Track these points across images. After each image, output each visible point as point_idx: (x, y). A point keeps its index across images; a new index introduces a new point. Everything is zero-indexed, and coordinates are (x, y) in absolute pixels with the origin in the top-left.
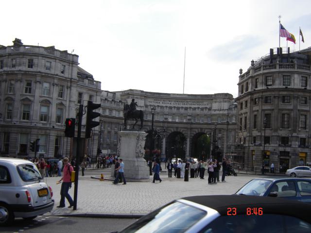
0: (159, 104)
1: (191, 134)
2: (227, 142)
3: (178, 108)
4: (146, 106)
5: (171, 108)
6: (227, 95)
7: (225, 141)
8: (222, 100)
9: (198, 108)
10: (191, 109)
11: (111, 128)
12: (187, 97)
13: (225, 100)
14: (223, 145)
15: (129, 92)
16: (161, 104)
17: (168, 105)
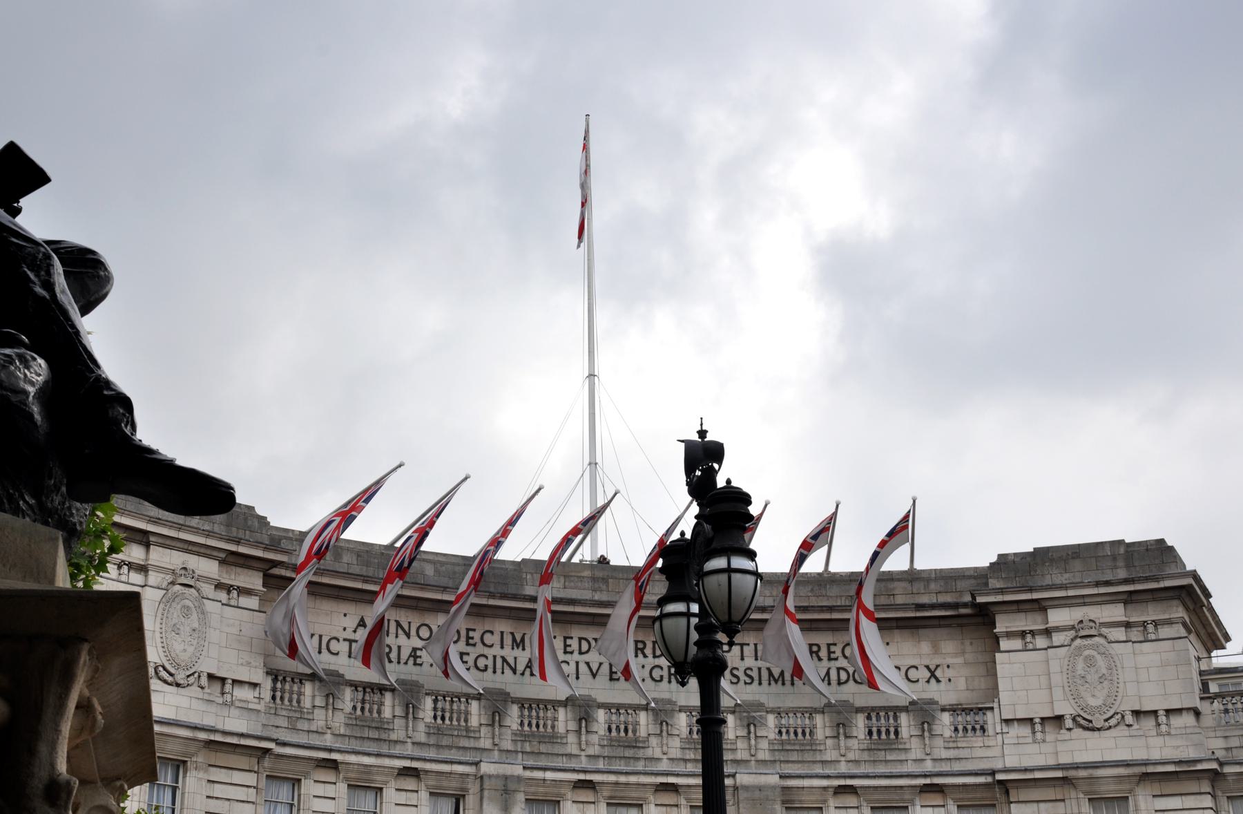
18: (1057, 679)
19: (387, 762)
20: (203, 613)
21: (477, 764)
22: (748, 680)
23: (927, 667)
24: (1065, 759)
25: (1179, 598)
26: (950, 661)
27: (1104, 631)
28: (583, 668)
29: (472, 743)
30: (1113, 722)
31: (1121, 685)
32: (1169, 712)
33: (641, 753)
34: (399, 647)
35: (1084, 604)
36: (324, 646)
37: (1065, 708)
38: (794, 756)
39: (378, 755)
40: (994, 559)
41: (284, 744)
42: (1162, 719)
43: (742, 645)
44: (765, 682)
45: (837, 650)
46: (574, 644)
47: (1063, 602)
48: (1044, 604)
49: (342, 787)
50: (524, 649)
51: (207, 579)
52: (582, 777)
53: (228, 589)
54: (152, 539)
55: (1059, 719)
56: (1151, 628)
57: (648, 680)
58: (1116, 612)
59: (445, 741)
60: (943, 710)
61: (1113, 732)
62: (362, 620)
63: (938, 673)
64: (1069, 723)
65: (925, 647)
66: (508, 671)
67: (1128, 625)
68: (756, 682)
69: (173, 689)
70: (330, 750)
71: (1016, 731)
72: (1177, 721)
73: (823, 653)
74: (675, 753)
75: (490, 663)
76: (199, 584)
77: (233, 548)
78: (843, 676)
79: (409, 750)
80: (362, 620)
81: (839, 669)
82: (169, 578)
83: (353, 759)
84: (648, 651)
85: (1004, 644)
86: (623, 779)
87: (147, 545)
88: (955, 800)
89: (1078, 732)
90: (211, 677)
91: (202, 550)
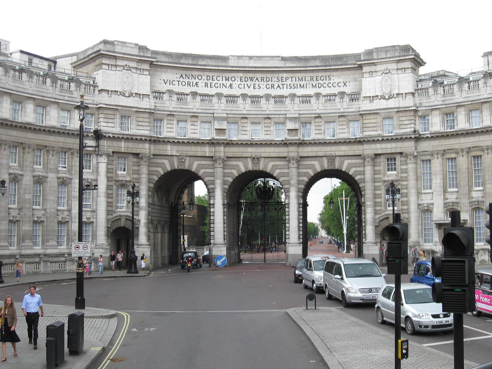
0: (194, 89)
1: (299, 175)
2: (419, 194)
3: (255, 99)
4: (158, 94)
5: (232, 99)
6: (407, 49)
7: (412, 193)
8: (393, 66)
9: (318, 95)
10: (297, 100)
11: (46, 168)
12: (278, 64)
13: (401, 65)
15: (101, 47)
16: (201, 89)
17: (226, 91)
21: (214, 114)
22: (294, 87)
23: (344, 82)
25: (411, 61)
28: (246, 86)
31: (394, 87)
32: (406, 94)
34: (193, 82)
35: (386, 64)
36: (171, 83)
39: (185, 112)
40: (364, 51)
42: (404, 96)
43: (292, 78)
45: (319, 78)
46: (243, 79)
47: (381, 63)
48: (375, 64)
50: (229, 81)
55: (377, 96)
62: (182, 75)
63: (346, 84)
68: (296, 88)
73: (315, 79)
75: (219, 85)
76: (131, 69)
78: (320, 85)
80: (182, 75)
81: (319, 84)
82: (123, 68)
84: (265, 80)
85: (365, 75)
87: (116, 59)
89: (382, 101)
91: (132, 60)
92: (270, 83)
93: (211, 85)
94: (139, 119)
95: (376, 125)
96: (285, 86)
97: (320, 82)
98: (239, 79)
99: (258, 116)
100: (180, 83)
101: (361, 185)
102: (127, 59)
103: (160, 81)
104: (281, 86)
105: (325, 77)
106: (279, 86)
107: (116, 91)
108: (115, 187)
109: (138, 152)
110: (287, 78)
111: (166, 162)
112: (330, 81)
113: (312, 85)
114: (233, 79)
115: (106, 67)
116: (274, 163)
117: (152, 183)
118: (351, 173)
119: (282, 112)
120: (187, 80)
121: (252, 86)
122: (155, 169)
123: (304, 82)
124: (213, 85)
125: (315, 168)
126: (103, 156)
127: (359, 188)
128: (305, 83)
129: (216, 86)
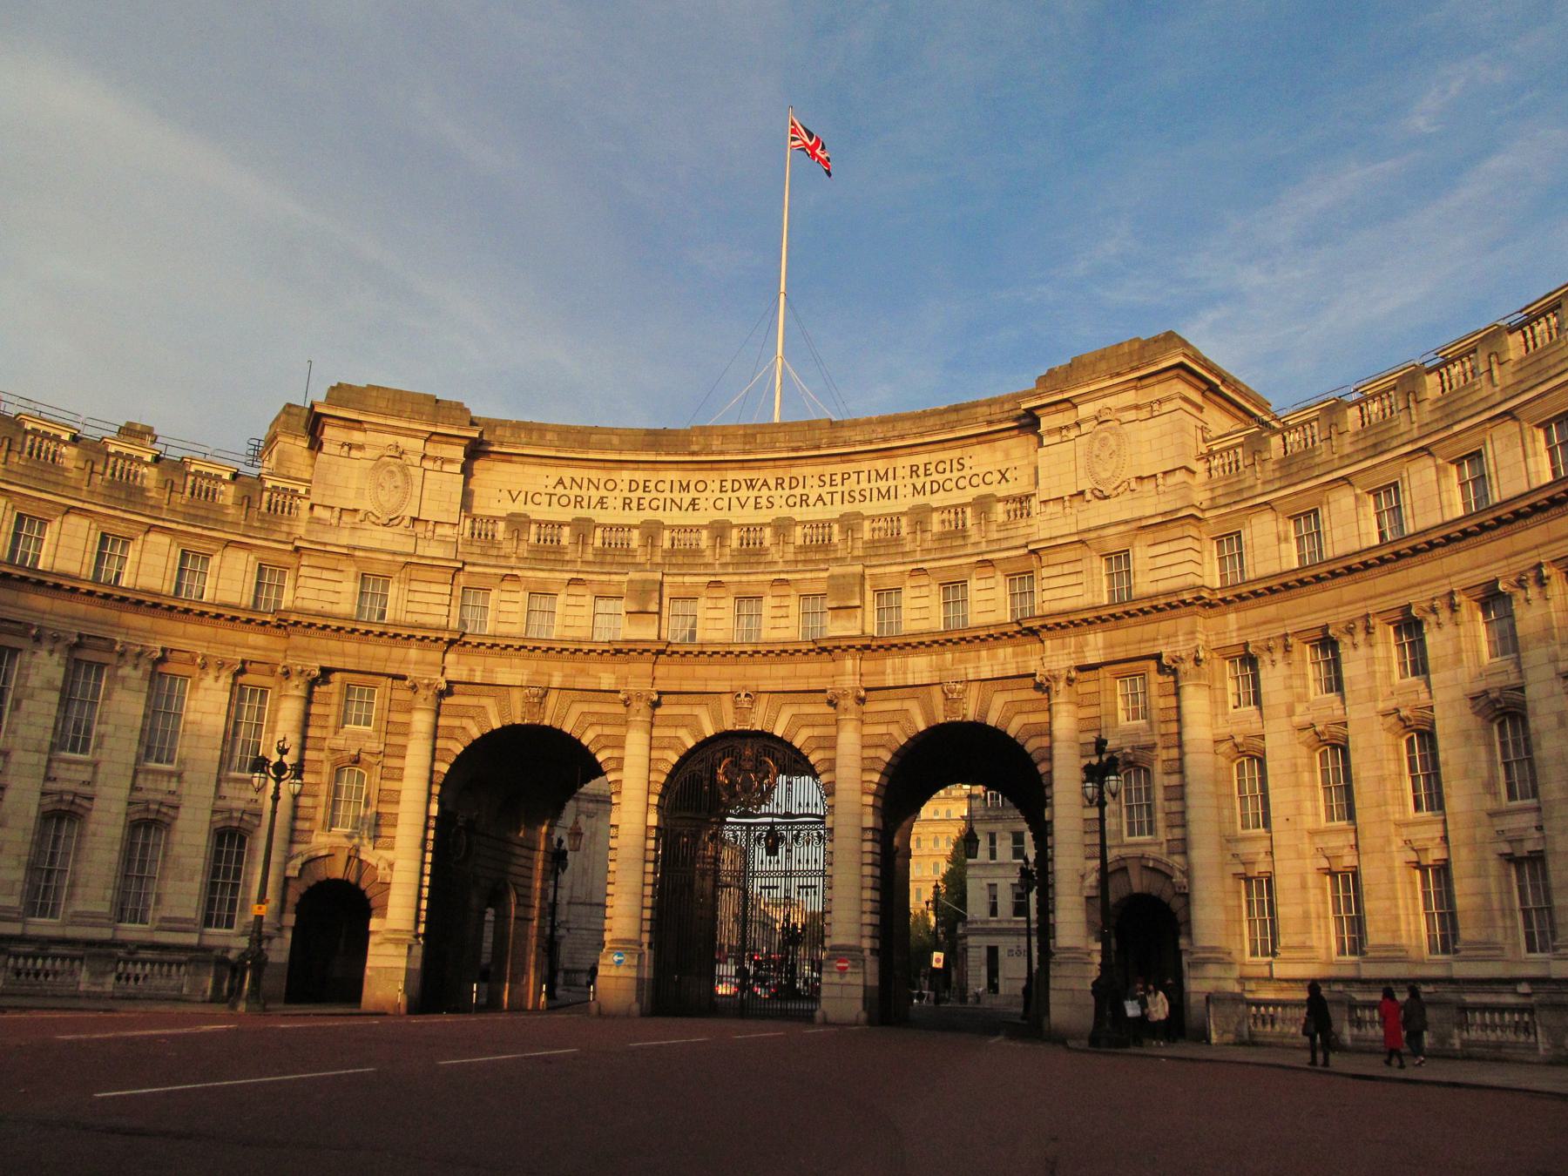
14: (1180, 820)
18: (1082, 461)
19: (557, 575)
20: (406, 475)
24: (1081, 527)
25: (1178, 376)
26: (1017, 464)
27: (1119, 415)
28: (734, 502)
29: (630, 560)
30: (1120, 490)
32: (1165, 473)
33: (762, 559)
35: (1105, 396)
37: (1086, 485)
38: (882, 551)
41: (474, 564)
44: (874, 499)
45: (932, 468)
46: (728, 485)
48: (1075, 401)
49: (522, 596)
51: (415, 452)
52: (713, 579)
53: (435, 459)
54: (366, 426)
55: (1082, 493)
56: (1156, 407)
57: (785, 507)
58: (1130, 397)
59: (609, 558)
60: (999, 500)
61: (1121, 498)
64: (1088, 496)
65: (999, 456)
66: (675, 508)
67: (1137, 407)
69: (381, 528)
70: (512, 568)
71: (1052, 507)
72: (1171, 480)
73: (921, 472)
74: (790, 557)
77: (433, 429)
78: (935, 487)
79: (579, 567)
83: (530, 574)
84: (786, 485)
86: (744, 578)
88: (1003, 571)
89: (1096, 502)
90: (414, 520)
92: (799, 491)
93: (639, 504)
94: (415, 586)
95: (1080, 578)
96: (837, 497)
97: (935, 477)
98: (717, 485)
99: (753, 578)
100: (555, 499)
101: (1042, 768)
102: (396, 431)
103: (500, 496)
104: (827, 498)
105: (948, 463)
106: (820, 498)
107: (356, 511)
108: (327, 768)
109: (402, 672)
110: (846, 476)
111: (488, 703)
112: (961, 474)
113: (915, 487)
114: (701, 486)
115: (334, 449)
116: (794, 710)
117: (443, 761)
118: (1011, 732)
119: (822, 566)
120: (576, 490)
121: (752, 501)
122: (456, 722)
123: (891, 482)
124: (645, 503)
125: (911, 722)
126: (294, 678)
127: (1039, 776)
128: (895, 483)
129: (654, 504)
